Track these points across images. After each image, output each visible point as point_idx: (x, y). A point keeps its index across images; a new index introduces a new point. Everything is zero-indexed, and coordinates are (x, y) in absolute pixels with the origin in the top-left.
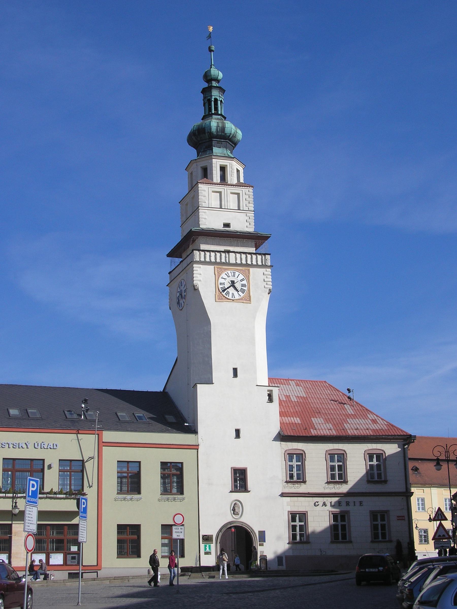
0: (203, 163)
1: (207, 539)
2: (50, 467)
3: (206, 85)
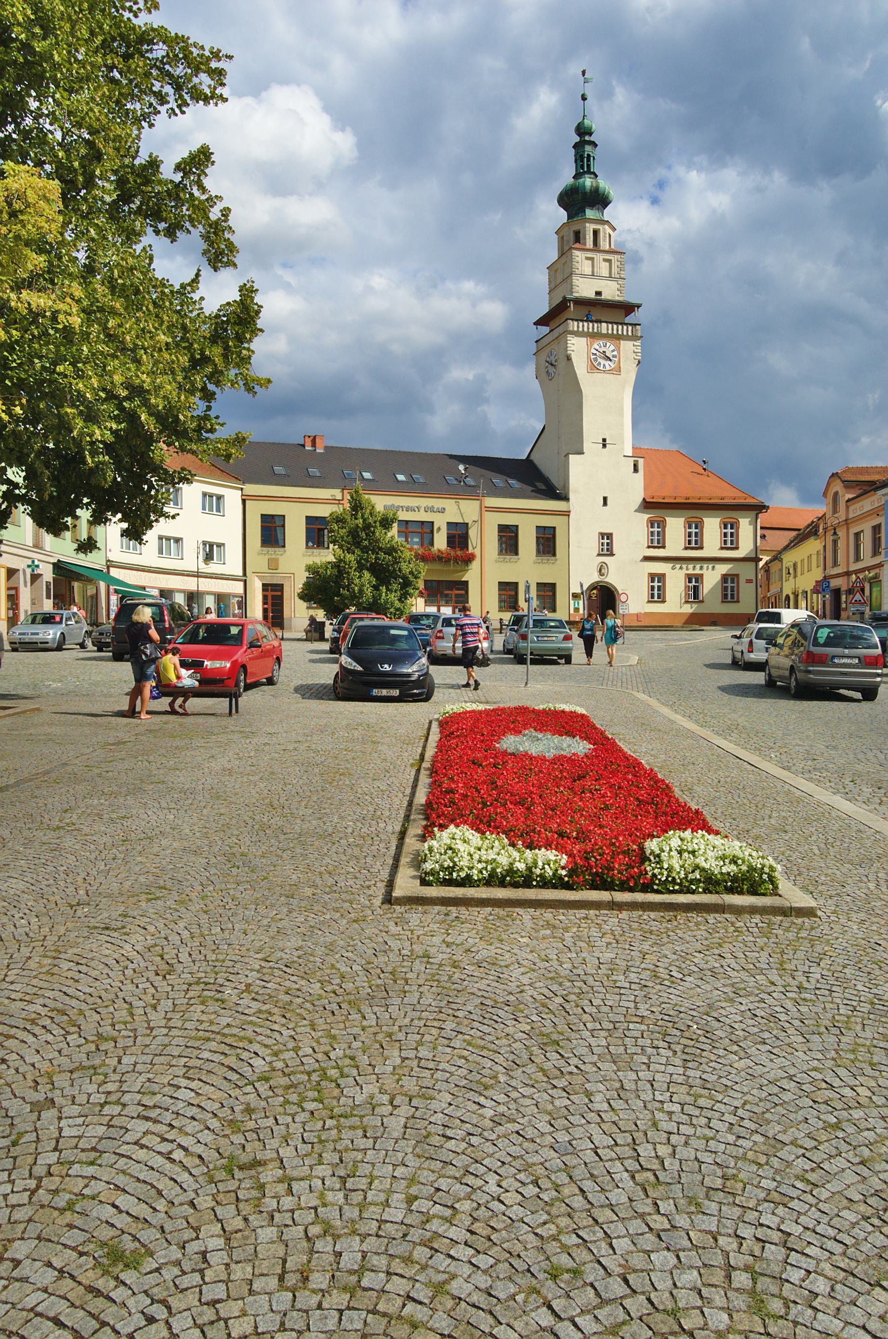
0: (576, 227)
3: (578, 139)
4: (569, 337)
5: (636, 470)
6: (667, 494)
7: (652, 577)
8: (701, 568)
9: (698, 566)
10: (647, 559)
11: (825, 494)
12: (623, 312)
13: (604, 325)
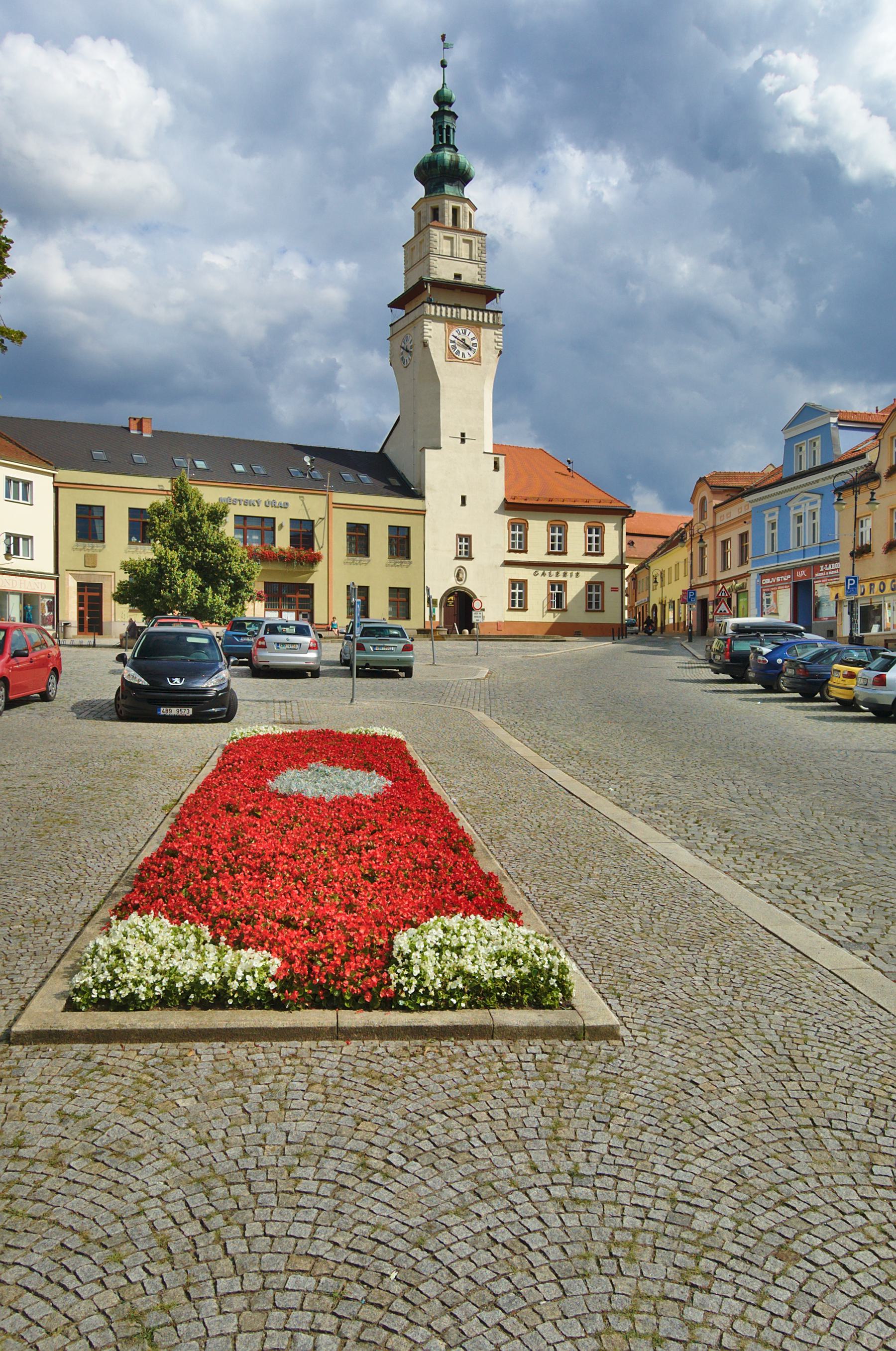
0: (434, 204)
2: (281, 526)
3: (437, 109)
4: (426, 322)
5: (496, 467)
6: (532, 495)
7: (513, 583)
9: (561, 573)
10: (507, 563)
11: (692, 500)
12: (484, 298)
13: (464, 310)
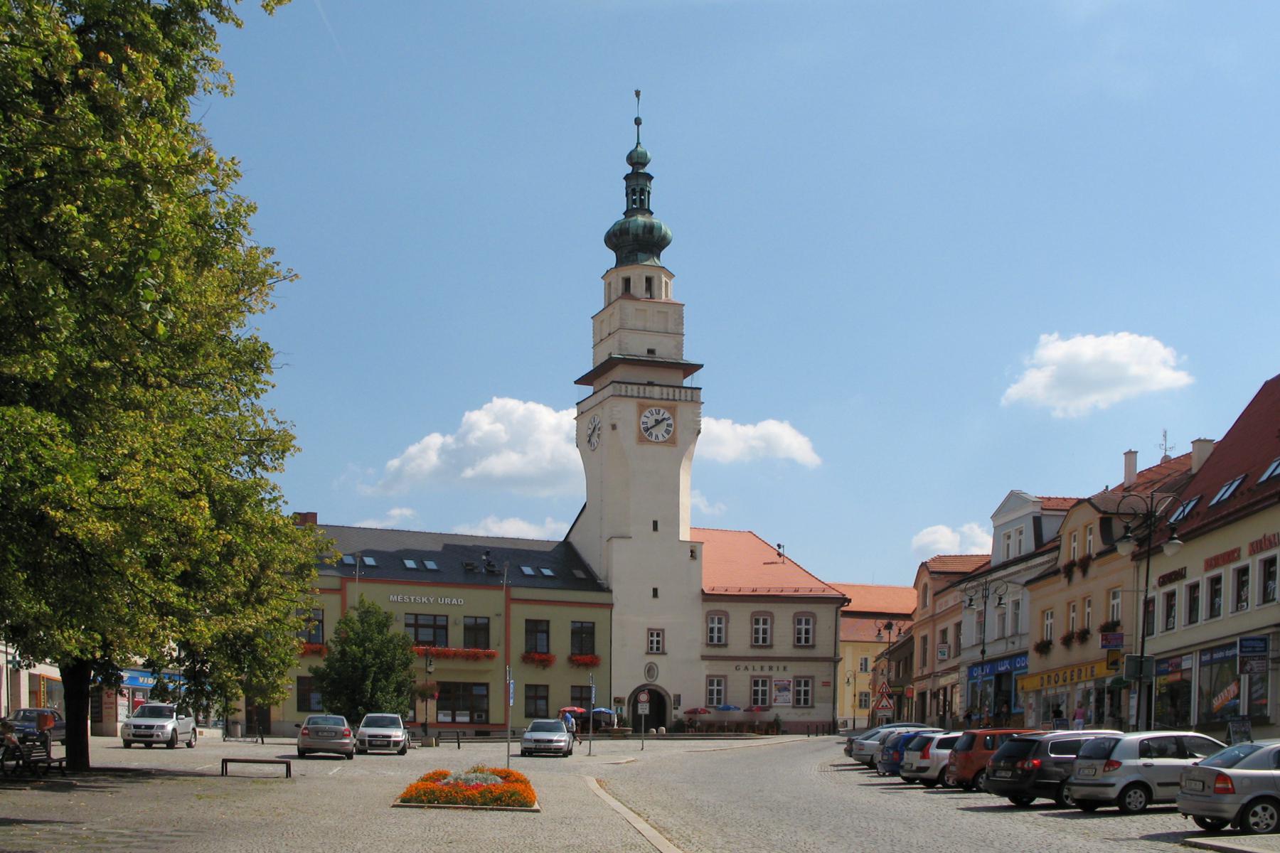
1: (619, 701)
8: (771, 668)
10: (704, 658)
12: (681, 374)
13: (657, 389)
